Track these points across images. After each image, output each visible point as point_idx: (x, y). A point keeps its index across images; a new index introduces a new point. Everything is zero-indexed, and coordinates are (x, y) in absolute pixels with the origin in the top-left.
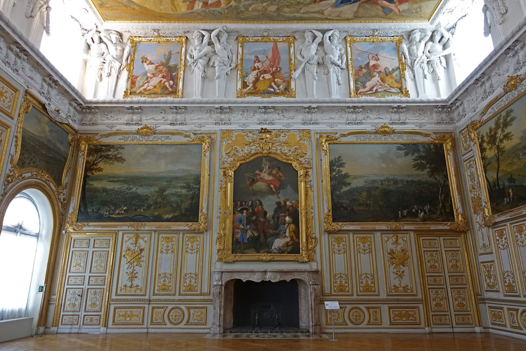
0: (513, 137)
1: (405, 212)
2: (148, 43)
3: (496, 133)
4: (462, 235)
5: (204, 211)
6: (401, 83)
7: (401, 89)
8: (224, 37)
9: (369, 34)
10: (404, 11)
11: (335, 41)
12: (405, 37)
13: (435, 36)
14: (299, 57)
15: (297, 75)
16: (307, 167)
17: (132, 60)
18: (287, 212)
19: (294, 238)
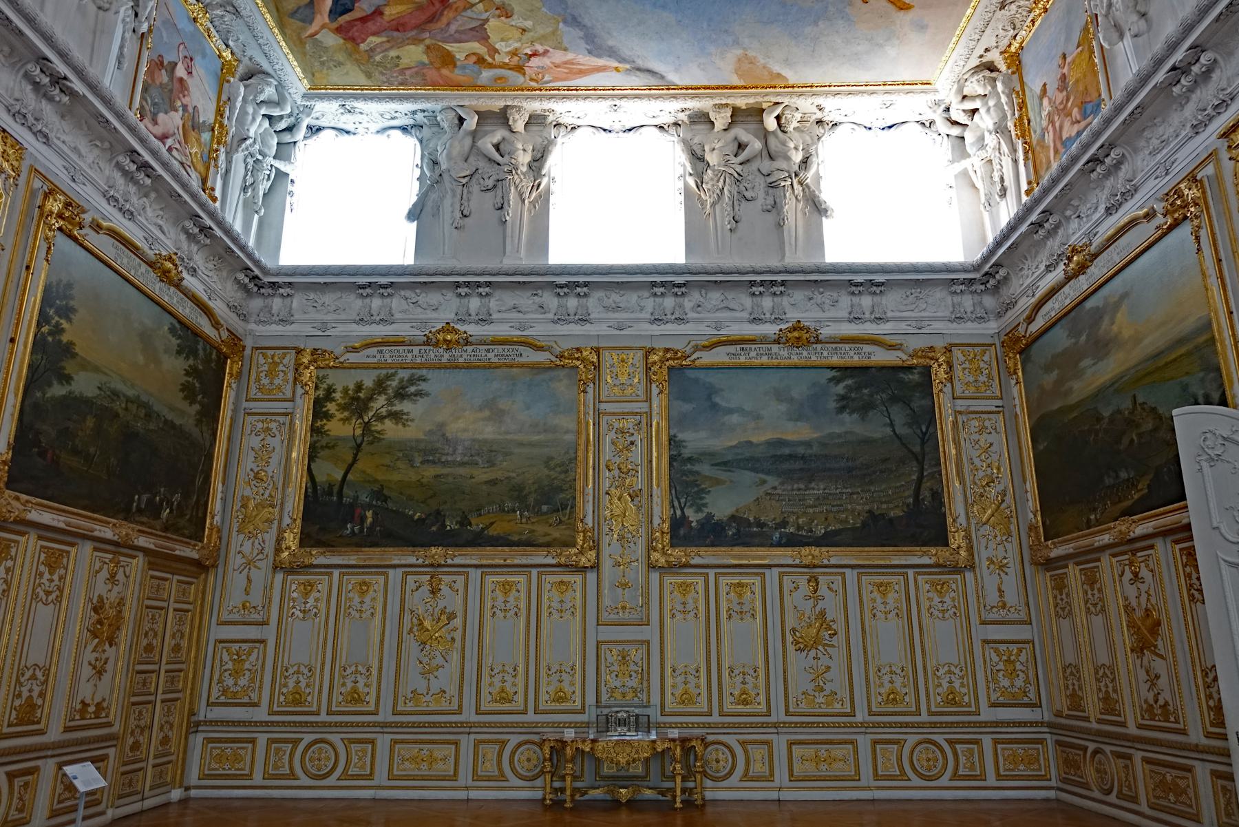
1: (145, 497)
3: (371, 399)
4: (203, 576)
12: (241, 70)
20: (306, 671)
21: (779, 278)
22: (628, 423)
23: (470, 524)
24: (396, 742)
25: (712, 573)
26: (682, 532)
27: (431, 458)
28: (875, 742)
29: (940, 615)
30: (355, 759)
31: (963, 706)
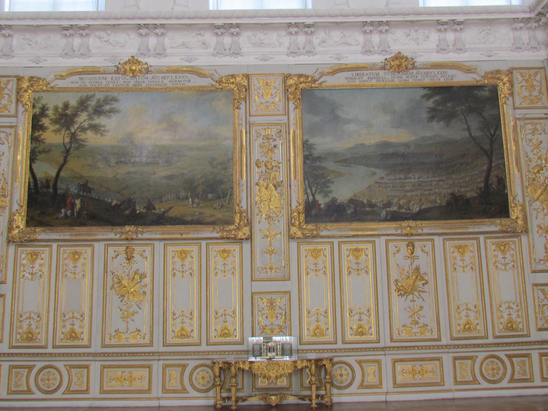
0: (106, 133)
3: (75, 115)
20: (36, 317)
21: (384, 19)
22: (272, 132)
23: (154, 209)
24: (104, 367)
25: (336, 241)
26: (313, 212)
27: (123, 159)
28: (455, 359)
29: (503, 267)
30: (75, 379)
31: (518, 331)
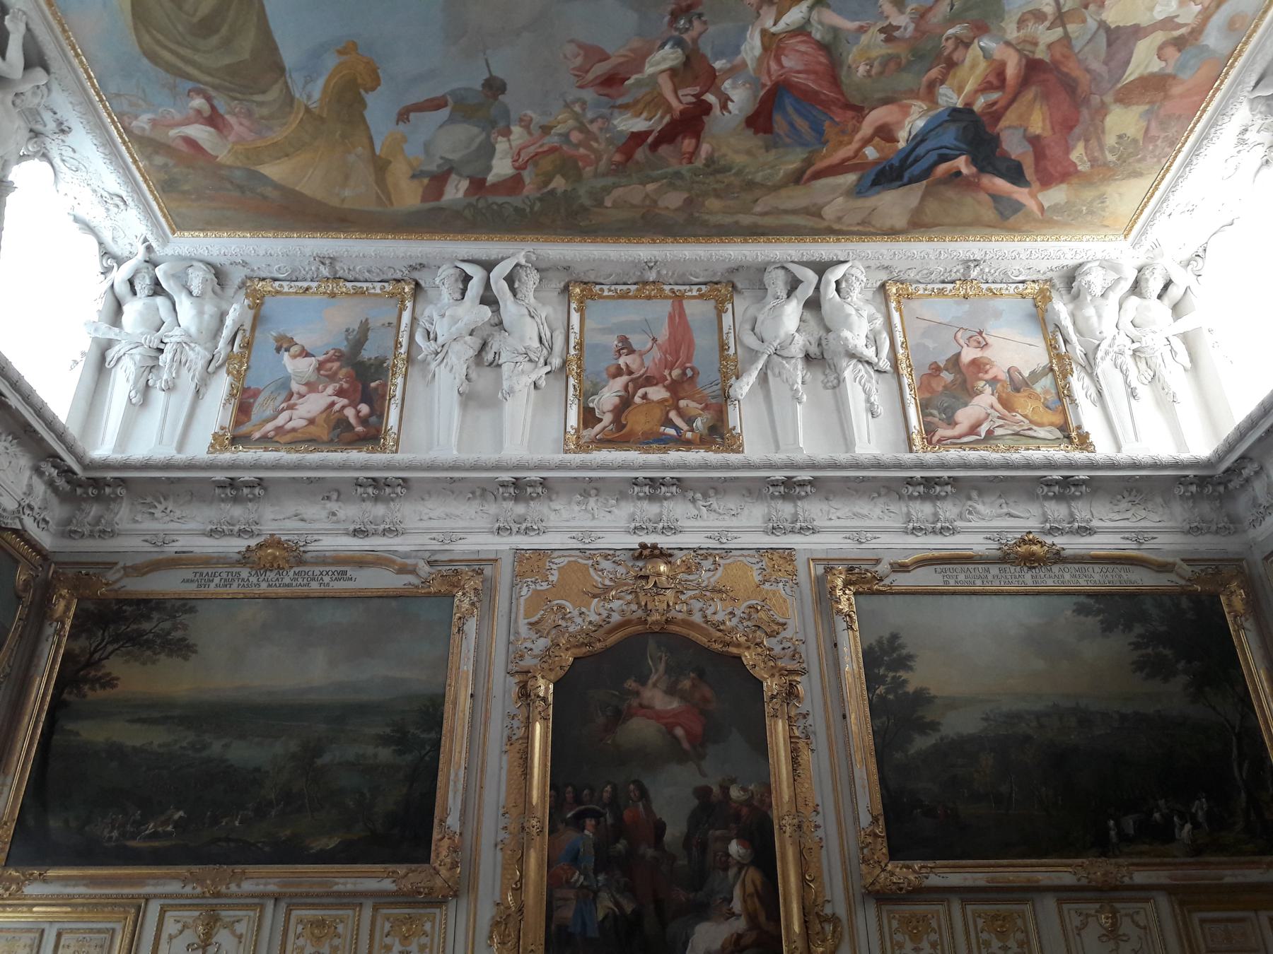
1: (1129, 823)
2: (298, 297)
5: (453, 821)
6: (1064, 412)
7: (1064, 428)
8: (530, 280)
9: (954, 276)
10: (1056, 208)
11: (856, 295)
13: (1147, 280)
14: (751, 340)
15: (746, 389)
16: (789, 667)
17: (248, 345)
18: (732, 825)
19: (762, 918)
